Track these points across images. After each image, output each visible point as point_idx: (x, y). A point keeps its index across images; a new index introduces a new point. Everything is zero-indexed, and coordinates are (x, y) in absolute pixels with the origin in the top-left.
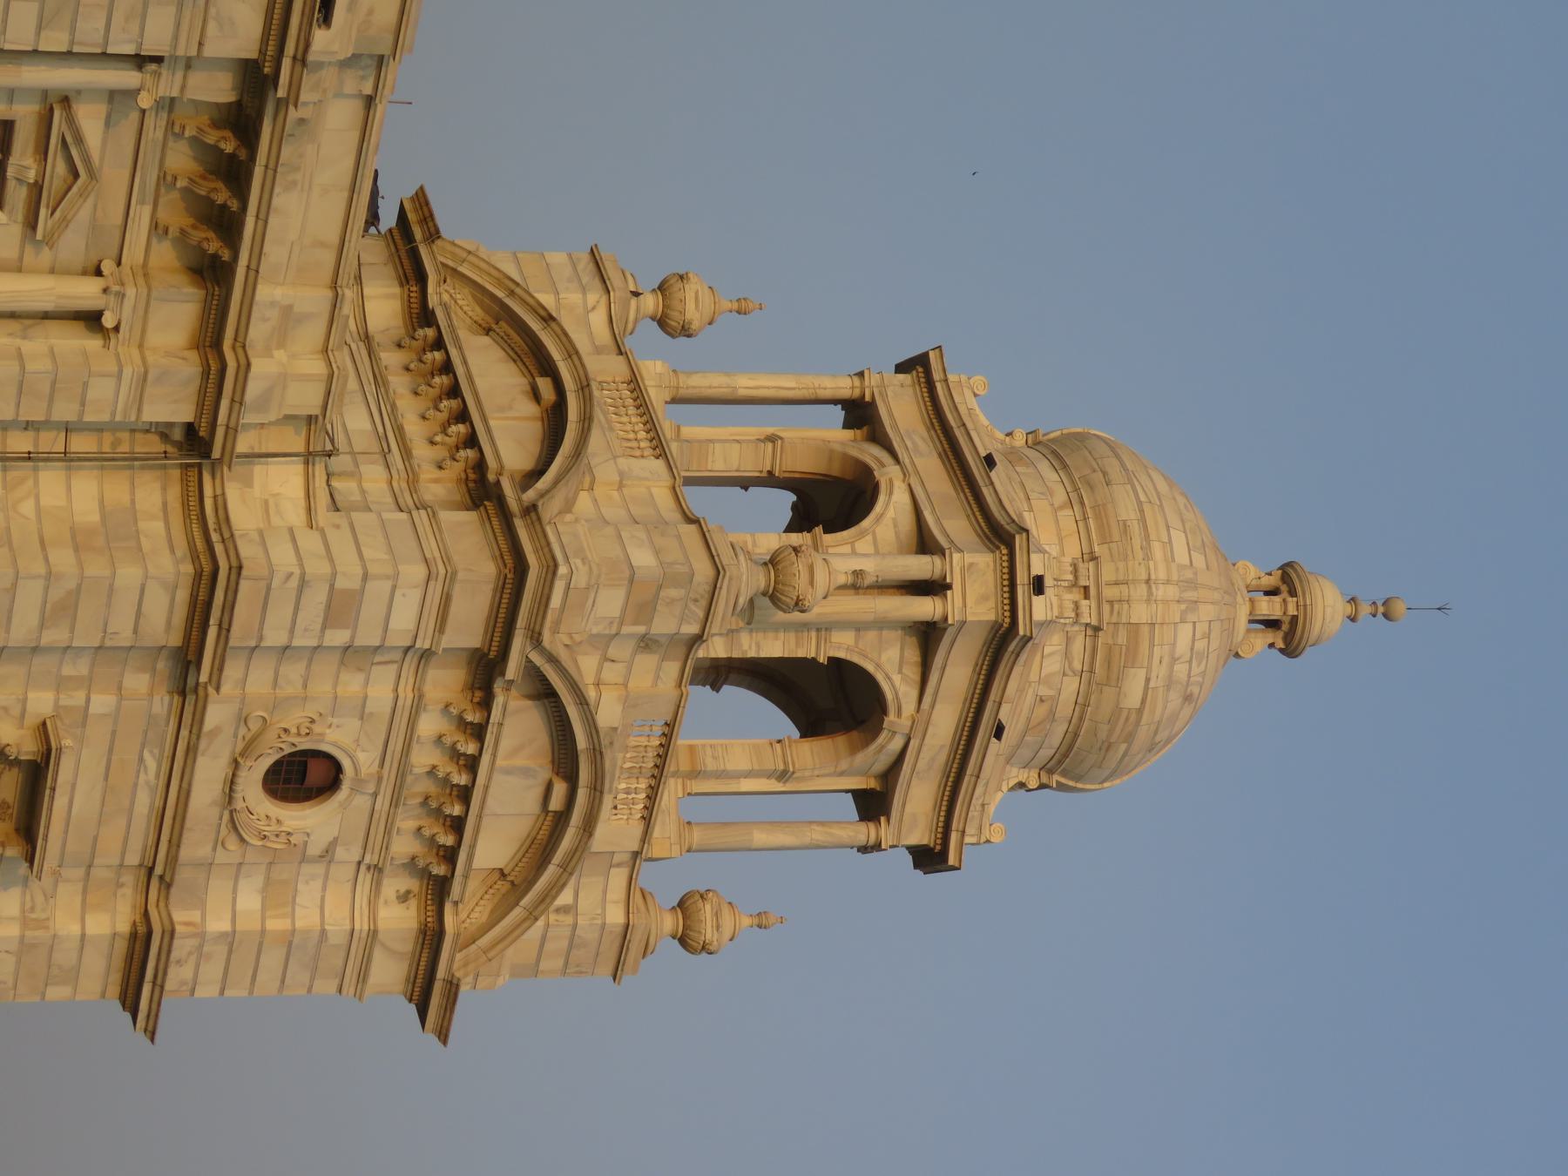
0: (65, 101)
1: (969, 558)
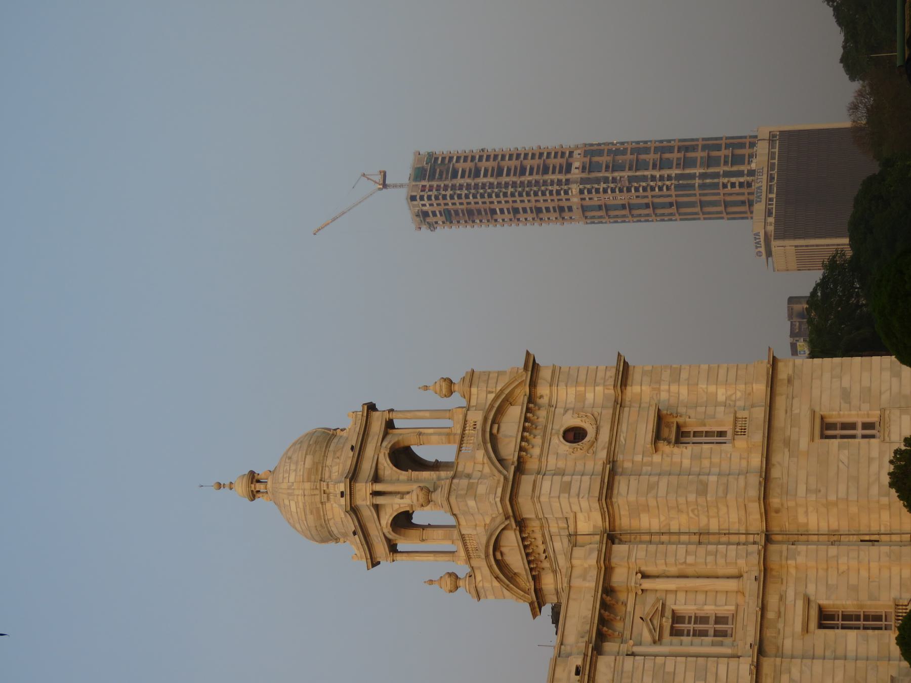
1: (364, 503)
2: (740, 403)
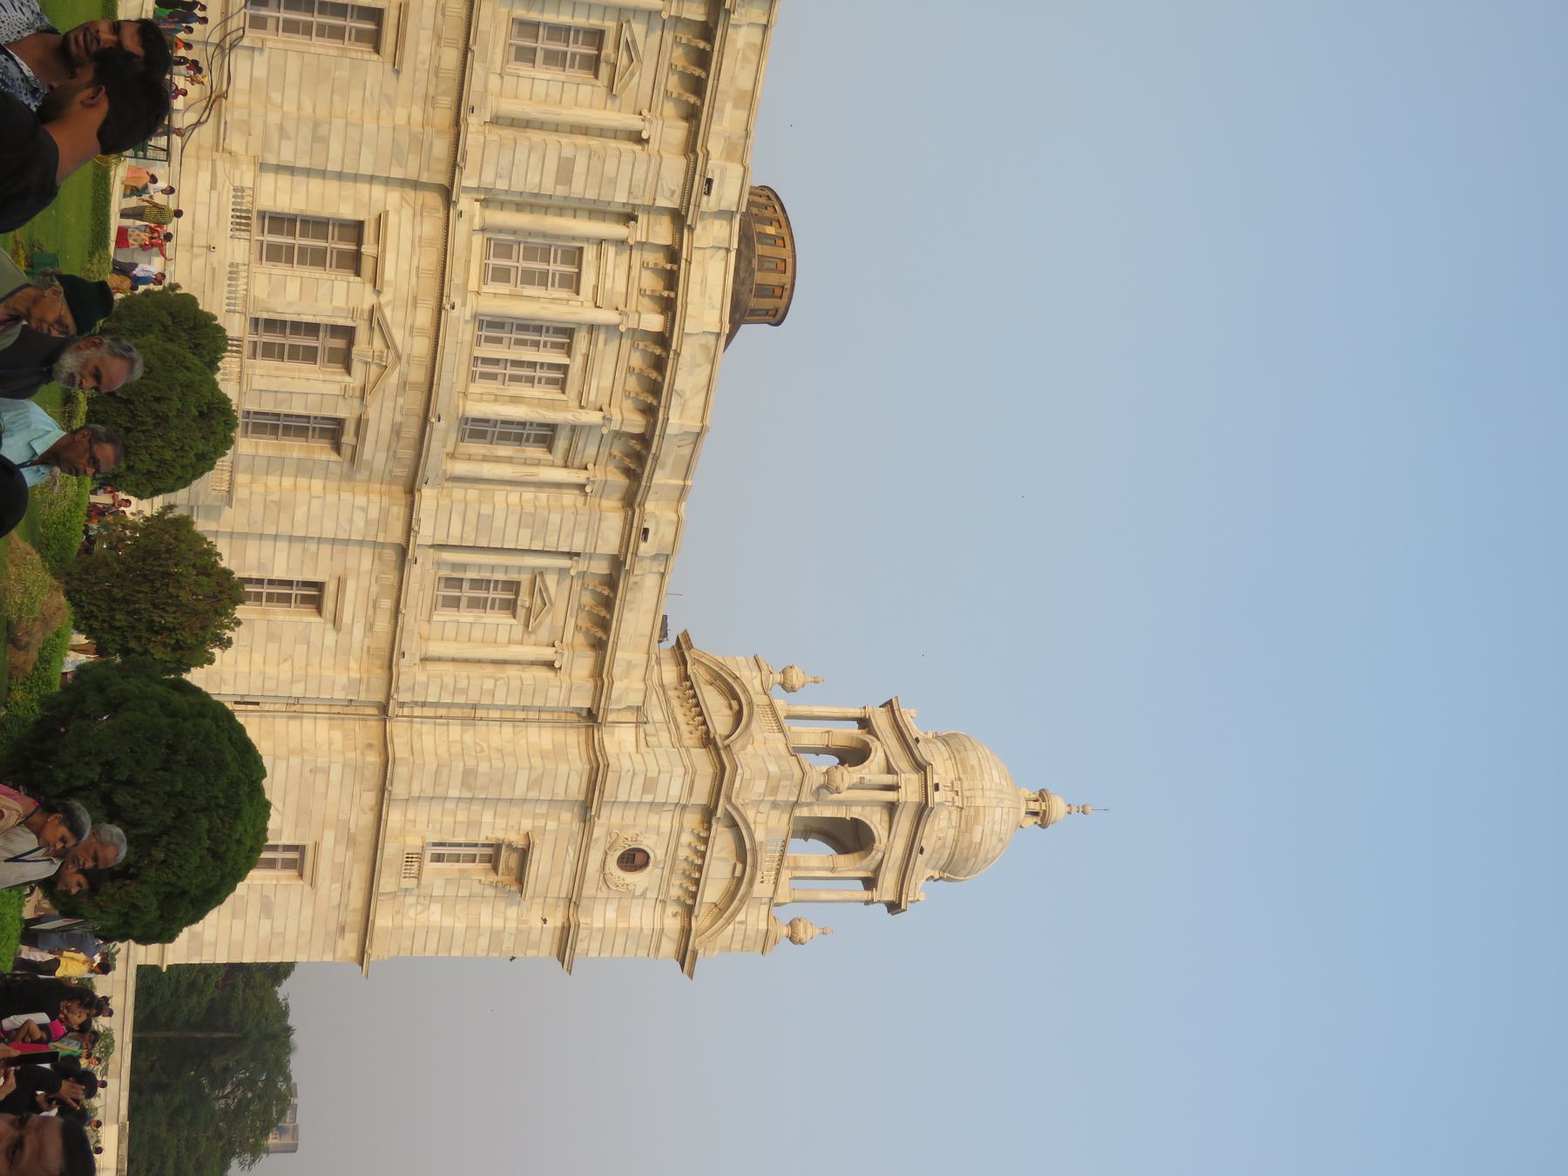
0: (541, 574)
1: (908, 776)
2: (410, 900)
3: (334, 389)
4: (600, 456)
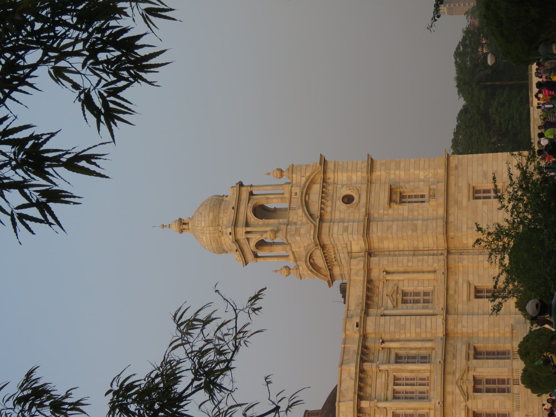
0: (394, 307)
1: (241, 237)
3: (478, 370)
4: (377, 353)
